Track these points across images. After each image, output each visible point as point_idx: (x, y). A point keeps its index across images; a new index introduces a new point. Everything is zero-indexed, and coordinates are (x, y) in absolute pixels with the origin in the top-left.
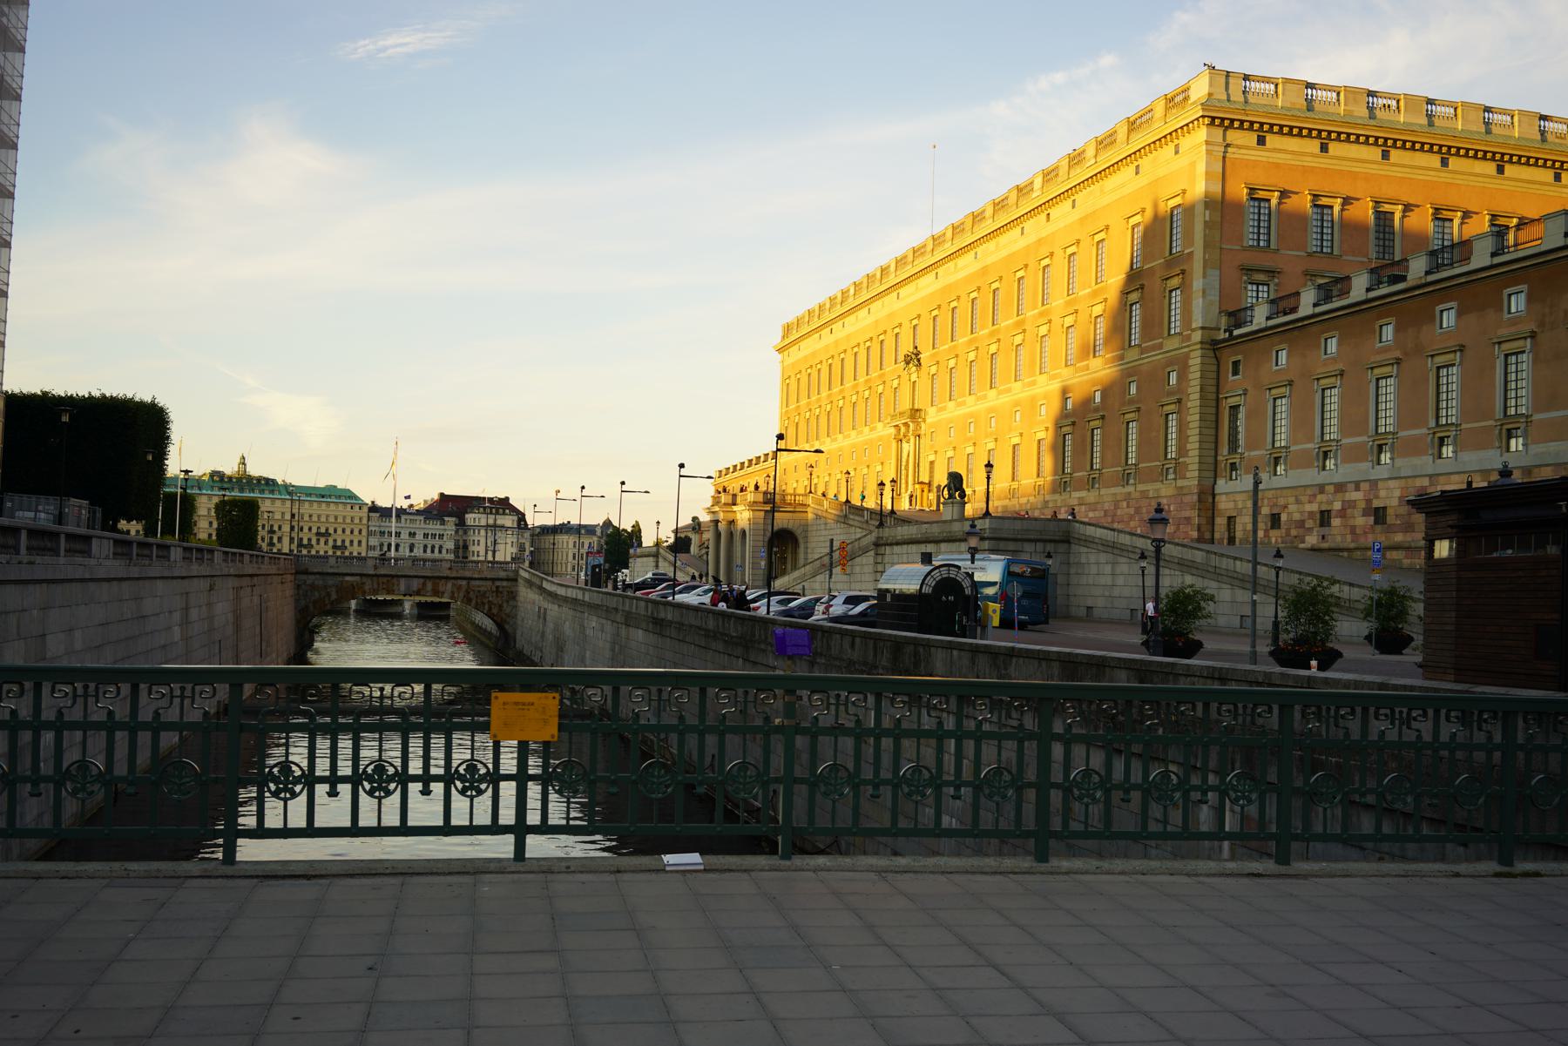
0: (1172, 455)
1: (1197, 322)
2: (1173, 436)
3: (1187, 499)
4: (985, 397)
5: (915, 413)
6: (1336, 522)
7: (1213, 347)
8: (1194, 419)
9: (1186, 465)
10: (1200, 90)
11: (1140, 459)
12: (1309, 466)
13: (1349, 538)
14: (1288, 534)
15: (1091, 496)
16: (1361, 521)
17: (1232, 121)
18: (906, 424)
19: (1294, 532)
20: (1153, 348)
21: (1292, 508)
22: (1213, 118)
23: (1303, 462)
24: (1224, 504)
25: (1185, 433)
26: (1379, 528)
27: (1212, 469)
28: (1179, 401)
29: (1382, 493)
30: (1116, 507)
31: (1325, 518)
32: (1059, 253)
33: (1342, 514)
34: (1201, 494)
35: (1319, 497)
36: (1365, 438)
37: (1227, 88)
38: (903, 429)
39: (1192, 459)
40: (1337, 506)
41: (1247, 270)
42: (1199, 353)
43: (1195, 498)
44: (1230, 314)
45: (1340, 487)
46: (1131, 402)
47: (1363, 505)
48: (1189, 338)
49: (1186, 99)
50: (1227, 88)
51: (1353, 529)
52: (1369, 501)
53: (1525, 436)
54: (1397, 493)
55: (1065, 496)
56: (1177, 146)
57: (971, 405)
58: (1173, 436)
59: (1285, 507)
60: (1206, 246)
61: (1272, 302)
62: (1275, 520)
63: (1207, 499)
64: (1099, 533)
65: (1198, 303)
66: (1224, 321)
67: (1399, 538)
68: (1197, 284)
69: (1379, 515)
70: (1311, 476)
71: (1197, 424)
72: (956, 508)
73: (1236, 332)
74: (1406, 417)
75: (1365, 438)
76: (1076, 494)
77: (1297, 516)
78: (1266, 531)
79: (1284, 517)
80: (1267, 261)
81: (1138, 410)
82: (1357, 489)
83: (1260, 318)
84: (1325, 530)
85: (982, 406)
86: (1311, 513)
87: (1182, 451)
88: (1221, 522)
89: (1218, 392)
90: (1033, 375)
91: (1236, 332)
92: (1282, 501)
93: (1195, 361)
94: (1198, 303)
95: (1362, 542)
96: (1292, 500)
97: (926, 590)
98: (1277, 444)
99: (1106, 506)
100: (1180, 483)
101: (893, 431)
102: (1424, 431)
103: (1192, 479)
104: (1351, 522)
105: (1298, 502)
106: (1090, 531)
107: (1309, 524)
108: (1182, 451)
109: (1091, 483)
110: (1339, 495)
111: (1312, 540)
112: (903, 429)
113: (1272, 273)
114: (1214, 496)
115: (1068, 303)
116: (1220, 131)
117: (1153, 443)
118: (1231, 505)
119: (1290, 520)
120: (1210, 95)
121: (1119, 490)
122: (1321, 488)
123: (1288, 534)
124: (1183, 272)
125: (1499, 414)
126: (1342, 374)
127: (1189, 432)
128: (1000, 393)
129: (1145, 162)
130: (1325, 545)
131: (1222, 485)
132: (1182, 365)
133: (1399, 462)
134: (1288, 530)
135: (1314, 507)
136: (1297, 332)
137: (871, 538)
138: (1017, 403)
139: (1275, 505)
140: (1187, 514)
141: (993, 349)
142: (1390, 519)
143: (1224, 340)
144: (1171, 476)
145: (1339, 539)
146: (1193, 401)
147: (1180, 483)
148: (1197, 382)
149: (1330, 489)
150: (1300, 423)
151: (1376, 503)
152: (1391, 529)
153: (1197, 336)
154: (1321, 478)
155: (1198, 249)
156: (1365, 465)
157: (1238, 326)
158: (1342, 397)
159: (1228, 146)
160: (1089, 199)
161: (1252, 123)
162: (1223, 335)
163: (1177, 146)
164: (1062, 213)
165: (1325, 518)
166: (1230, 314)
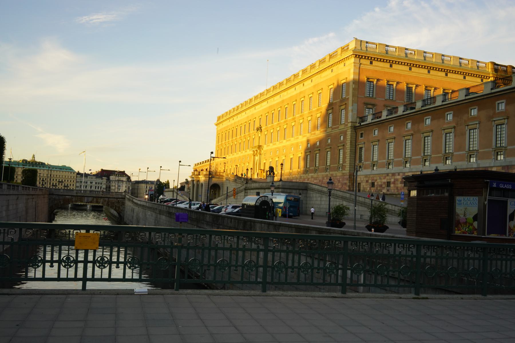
1: (350, 120)
8: (348, 151)
12: (384, 167)
14: (377, 189)
19: (379, 188)
23: (382, 166)
28: (344, 145)
31: (388, 184)
35: (387, 177)
39: (347, 164)
43: (348, 177)
62: (373, 184)
77: (380, 183)
79: (376, 184)
81: (331, 148)
86: (384, 183)
89: (356, 143)
93: (349, 133)
100: (344, 172)
103: (347, 171)
105: (380, 179)
107: (384, 186)
108: (344, 161)
122: (388, 175)
123: (377, 189)
126: (395, 138)
132: (345, 133)
140: (345, 182)
146: (348, 146)
147: (344, 172)
153: (350, 125)
155: (350, 97)
158: (395, 145)
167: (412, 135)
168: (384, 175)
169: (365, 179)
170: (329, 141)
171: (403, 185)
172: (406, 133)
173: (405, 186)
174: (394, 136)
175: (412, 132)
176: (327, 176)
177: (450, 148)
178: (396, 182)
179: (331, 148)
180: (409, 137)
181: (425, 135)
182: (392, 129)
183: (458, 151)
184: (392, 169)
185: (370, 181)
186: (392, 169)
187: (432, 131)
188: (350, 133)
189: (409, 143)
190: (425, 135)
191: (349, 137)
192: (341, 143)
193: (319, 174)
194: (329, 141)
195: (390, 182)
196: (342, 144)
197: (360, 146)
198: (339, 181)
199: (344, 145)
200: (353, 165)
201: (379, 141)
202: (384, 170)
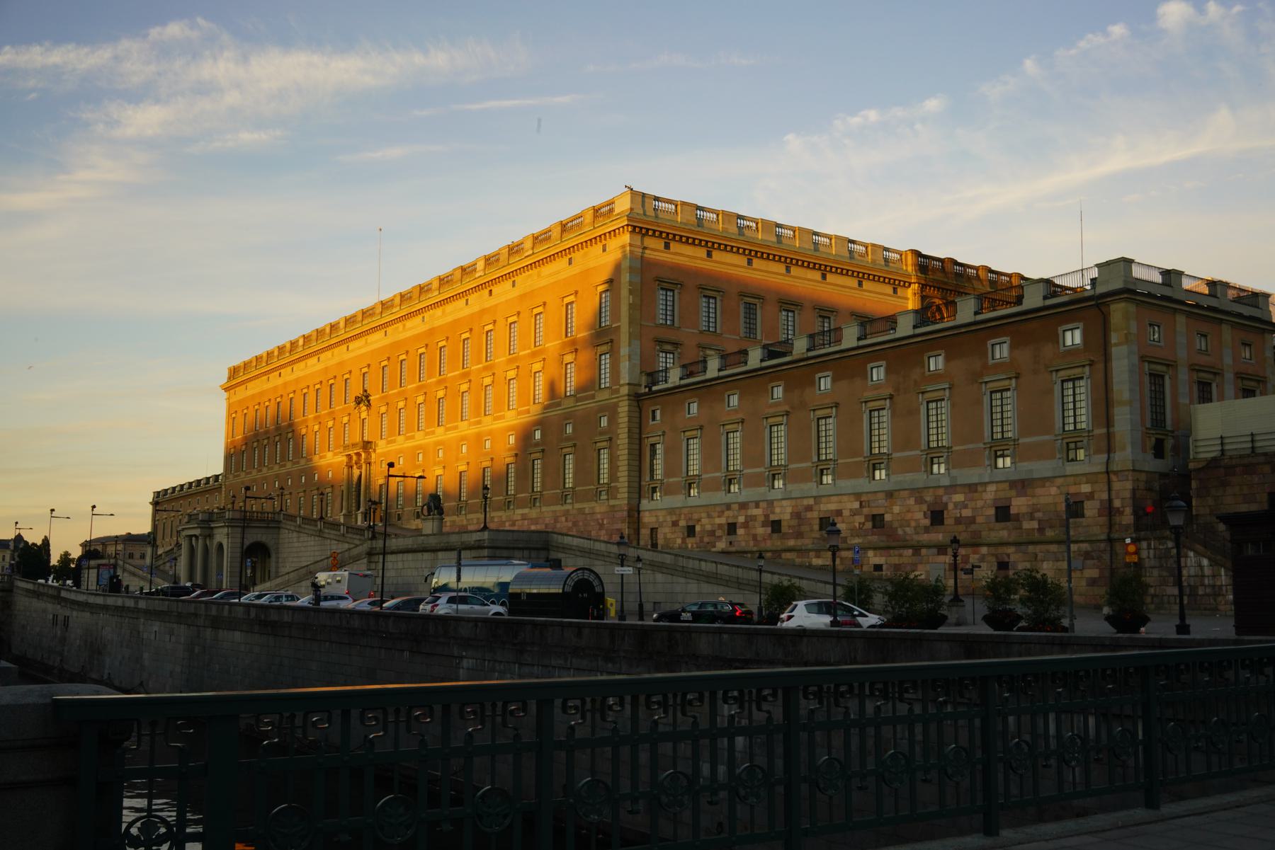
0: (604, 478)
2: (605, 466)
3: (618, 515)
4: (433, 432)
5: (367, 445)
6: (740, 531)
7: (637, 399)
8: (623, 454)
9: (617, 488)
10: (623, 205)
11: (576, 483)
13: (752, 543)
14: (701, 541)
15: (533, 513)
16: (761, 531)
17: (648, 230)
18: (358, 455)
19: (706, 540)
20: (586, 398)
21: (705, 521)
22: (635, 227)
24: (647, 518)
25: (612, 465)
26: (775, 535)
27: (639, 491)
29: (777, 510)
30: (556, 520)
32: (501, 322)
33: (746, 525)
34: (629, 511)
35: (727, 513)
36: (762, 469)
37: (643, 206)
38: (355, 458)
40: (741, 519)
41: (660, 342)
42: (626, 403)
43: (625, 514)
44: (650, 375)
45: (743, 506)
46: (568, 439)
47: (762, 518)
48: (617, 391)
49: (611, 211)
50: (643, 206)
51: (755, 537)
52: (767, 516)
53: (887, 469)
54: (789, 510)
55: (509, 513)
56: (604, 246)
57: (420, 439)
58: (605, 466)
59: (699, 520)
60: (631, 323)
61: (684, 366)
63: (634, 514)
64: (576, 542)
65: (625, 366)
66: (644, 380)
67: (791, 543)
68: (624, 351)
69: (776, 526)
70: (719, 497)
71: (626, 457)
72: (436, 523)
73: (654, 388)
74: (795, 453)
75: (762, 469)
76: (520, 511)
77: (708, 527)
78: (683, 539)
79: (698, 528)
80: (672, 336)
81: (575, 445)
82: (757, 506)
83: (674, 378)
84: (732, 538)
85: (431, 439)
87: (613, 476)
88: (645, 532)
89: (640, 433)
90: (478, 415)
91: (654, 388)
92: (696, 516)
94: (625, 366)
95: (763, 546)
96: (704, 515)
97: (568, 589)
98: (691, 473)
99: (547, 520)
101: (345, 459)
102: (809, 464)
104: (753, 531)
105: (709, 516)
106: (567, 540)
109: (533, 502)
110: (743, 512)
111: (721, 545)
112: (355, 458)
113: (676, 344)
114: (639, 512)
115: (510, 361)
116: (638, 238)
117: (587, 472)
118: (654, 519)
119: (703, 531)
120: (631, 209)
121: (558, 508)
122: (728, 507)
123: (701, 541)
124: (612, 341)
125: (866, 453)
126: (742, 422)
127: (619, 463)
128: (447, 430)
129: (576, 256)
130: (733, 549)
131: (645, 504)
133: (790, 487)
134: (702, 538)
135: (723, 520)
136: (709, 390)
137: (366, 547)
138: (463, 438)
139: (690, 519)
140: (619, 526)
141: (441, 394)
143: (645, 394)
144: (604, 497)
145: (743, 544)
146: (623, 439)
148: (625, 425)
150: (709, 457)
151: (773, 518)
154: (728, 499)
156: (763, 490)
157: (655, 384)
158: (743, 438)
159: (645, 248)
160: (526, 282)
161: (661, 233)
162: (644, 390)
163: (604, 246)
164: (504, 292)
165: (732, 528)
166: (650, 375)
167: (787, 413)
169: (669, 519)
170: (569, 429)
172: (771, 411)
174: (741, 416)
175: (787, 408)
176: (566, 513)
177: (883, 443)
180: (780, 419)
181: (820, 413)
182: (734, 400)
183: (903, 450)
185: (682, 523)
187: (837, 405)
189: (781, 432)
190: (820, 413)
191: (623, 419)
192: (601, 434)
194: (569, 429)
196: (606, 437)
197: (652, 440)
198: (601, 526)
199: (610, 439)
201: (701, 428)
202: (719, 497)
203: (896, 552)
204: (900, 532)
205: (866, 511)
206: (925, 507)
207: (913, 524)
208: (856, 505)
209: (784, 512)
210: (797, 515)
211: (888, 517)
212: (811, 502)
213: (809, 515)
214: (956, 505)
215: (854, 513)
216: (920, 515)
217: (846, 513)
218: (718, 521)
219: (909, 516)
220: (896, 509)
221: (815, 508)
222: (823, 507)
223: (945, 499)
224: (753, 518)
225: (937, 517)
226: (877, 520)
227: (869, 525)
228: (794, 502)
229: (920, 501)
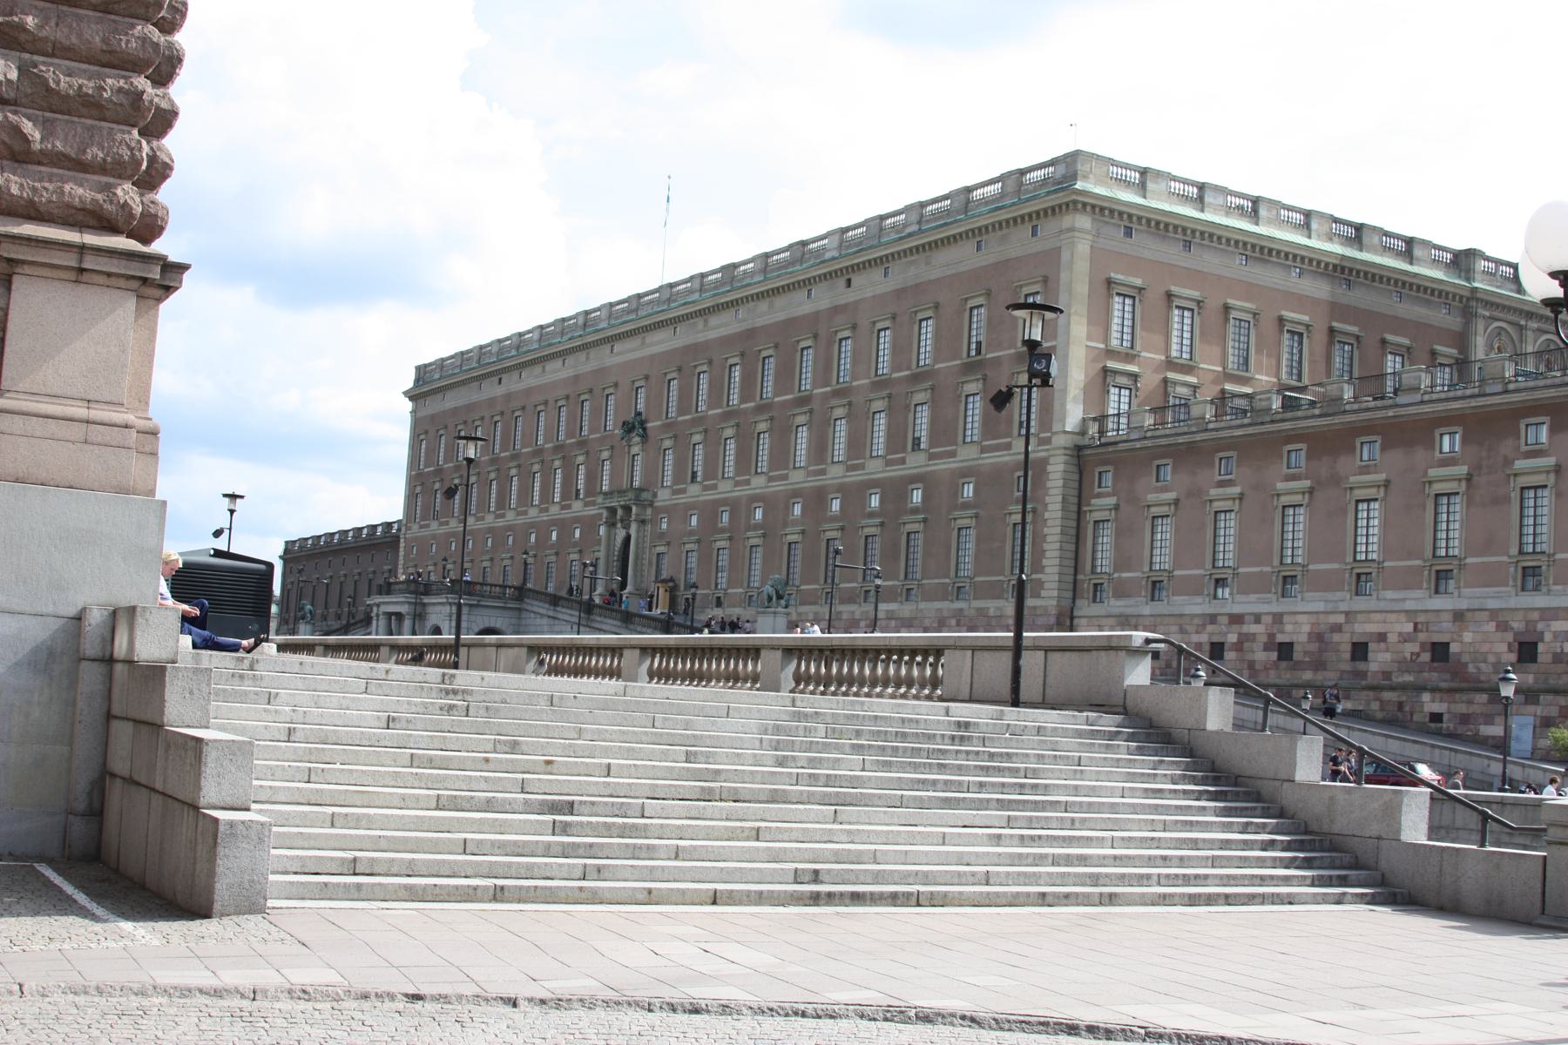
6: (1229, 655)
9: (1040, 583)
12: (1198, 592)
16: (1261, 656)
26: (1284, 664)
29: (1289, 628)
33: (1238, 647)
35: (1210, 628)
40: (1232, 638)
45: (1236, 619)
47: (1264, 639)
52: (1271, 636)
54: (1306, 628)
56: (1034, 228)
67: (1308, 676)
81: (977, 516)
86: (1199, 646)
104: (1249, 657)
105: (1182, 631)
110: (1235, 627)
122: (1213, 619)
127: (1046, 546)
135: (1204, 638)
142: (1297, 656)
148: (1058, 491)
149: (1225, 620)
151: (1280, 638)
152: (1297, 666)
163: (1034, 228)
165: (1217, 650)
168: (1197, 621)
170: (969, 491)
171: (1274, 655)
173: (1279, 658)
178: (1246, 645)
179: (977, 516)
184: (1232, 601)
186: (1232, 601)
188: (1061, 467)
193: (922, 605)
195: (1222, 644)
200: (1071, 579)
202: (1197, 606)
203: (1465, 697)
204: (1471, 669)
205: (1422, 636)
206: (1510, 637)
207: (1491, 659)
208: (1409, 628)
209: (1297, 631)
210: (1318, 637)
211: (1454, 648)
212: (1341, 619)
213: (1336, 637)
214: (1556, 635)
215: (1405, 638)
216: (1504, 648)
217: (1392, 638)
218: (1195, 638)
219: (1485, 648)
220: (1468, 637)
221: (1346, 628)
222: (1358, 628)
223: (1540, 626)
224: (1251, 637)
225: (1527, 651)
226: (1440, 651)
227: (1426, 657)
228: (1313, 619)
229: (1503, 627)
